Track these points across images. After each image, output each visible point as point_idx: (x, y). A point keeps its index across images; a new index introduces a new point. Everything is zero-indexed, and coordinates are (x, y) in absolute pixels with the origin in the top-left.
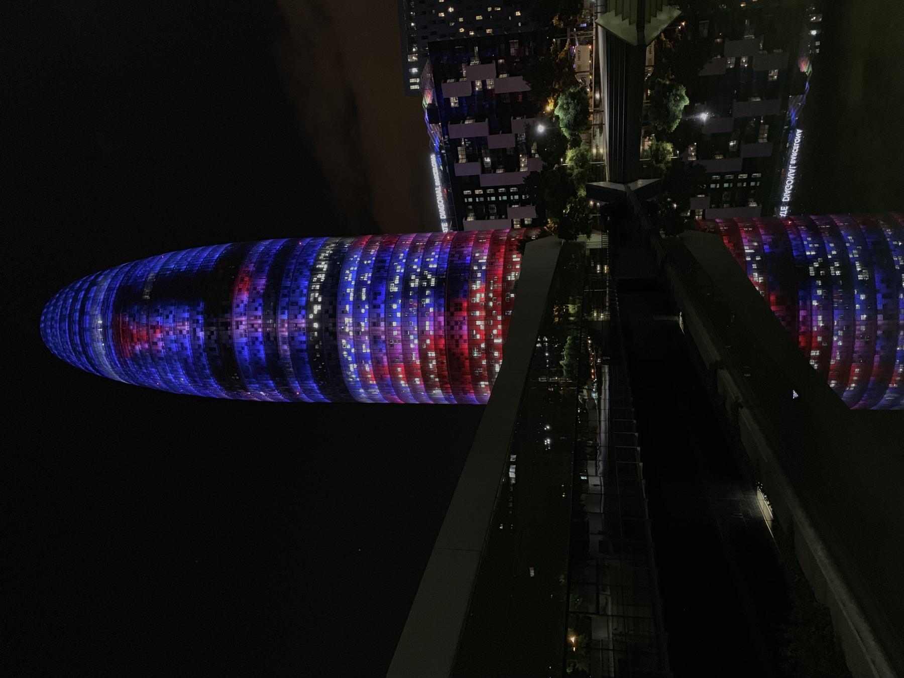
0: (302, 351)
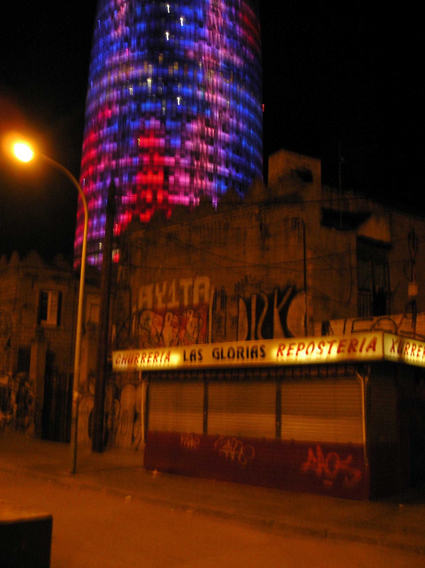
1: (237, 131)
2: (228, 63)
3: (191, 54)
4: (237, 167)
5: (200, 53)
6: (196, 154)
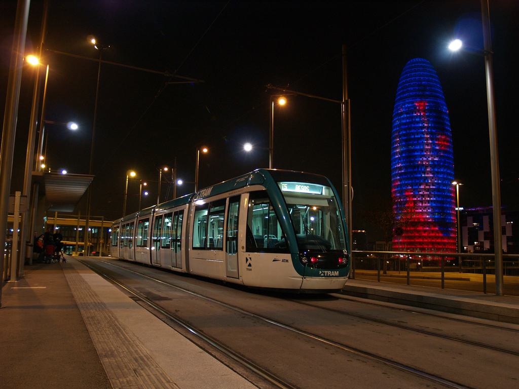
0: (418, 168)
1: (438, 184)
2: (433, 161)
3: (419, 162)
4: (439, 196)
5: (422, 161)
6: (423, 196)
